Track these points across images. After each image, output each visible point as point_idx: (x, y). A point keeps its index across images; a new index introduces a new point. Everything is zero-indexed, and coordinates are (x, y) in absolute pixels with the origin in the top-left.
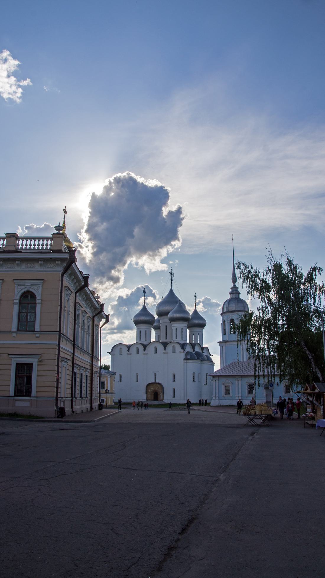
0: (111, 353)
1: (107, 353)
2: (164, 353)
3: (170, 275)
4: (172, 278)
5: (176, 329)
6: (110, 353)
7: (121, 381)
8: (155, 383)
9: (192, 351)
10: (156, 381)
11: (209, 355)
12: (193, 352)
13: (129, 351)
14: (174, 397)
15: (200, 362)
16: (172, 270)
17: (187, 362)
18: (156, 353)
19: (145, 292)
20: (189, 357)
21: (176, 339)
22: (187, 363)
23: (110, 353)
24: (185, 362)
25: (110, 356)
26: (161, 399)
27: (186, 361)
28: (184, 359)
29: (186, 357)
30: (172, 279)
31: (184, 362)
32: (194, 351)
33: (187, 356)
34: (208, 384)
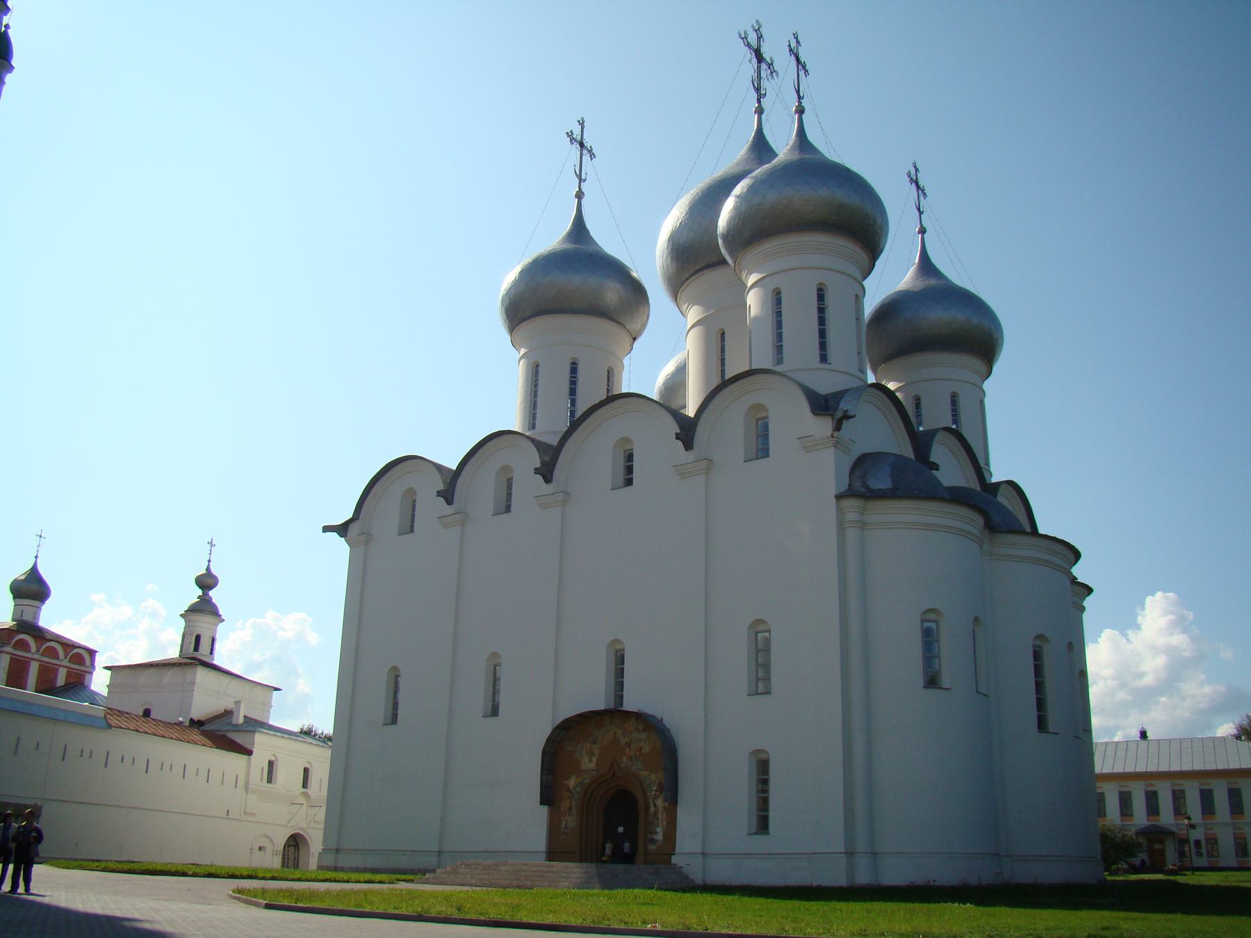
0: (353, 529)
1: (327, 529)
2: (683, 472)
3: (749, 55)
4: (759, 78)
6: (342, 530)
7: (394, 720)
8: (615, 714)
10: (619, 698)
13: (448, 495)
14: (763, 825)
15: (977, 533)
16: (760, 37)
18: (629, 482)
19: (582, 145)
21: (780, 361)
22: (863, 526)
23: (342, 530)
24: (851, 516)
25: (340, 548)
26: (652, 847)
28: (839, 497)
29: (857, 485)
30: (765, 84)
34: (1051, 728)
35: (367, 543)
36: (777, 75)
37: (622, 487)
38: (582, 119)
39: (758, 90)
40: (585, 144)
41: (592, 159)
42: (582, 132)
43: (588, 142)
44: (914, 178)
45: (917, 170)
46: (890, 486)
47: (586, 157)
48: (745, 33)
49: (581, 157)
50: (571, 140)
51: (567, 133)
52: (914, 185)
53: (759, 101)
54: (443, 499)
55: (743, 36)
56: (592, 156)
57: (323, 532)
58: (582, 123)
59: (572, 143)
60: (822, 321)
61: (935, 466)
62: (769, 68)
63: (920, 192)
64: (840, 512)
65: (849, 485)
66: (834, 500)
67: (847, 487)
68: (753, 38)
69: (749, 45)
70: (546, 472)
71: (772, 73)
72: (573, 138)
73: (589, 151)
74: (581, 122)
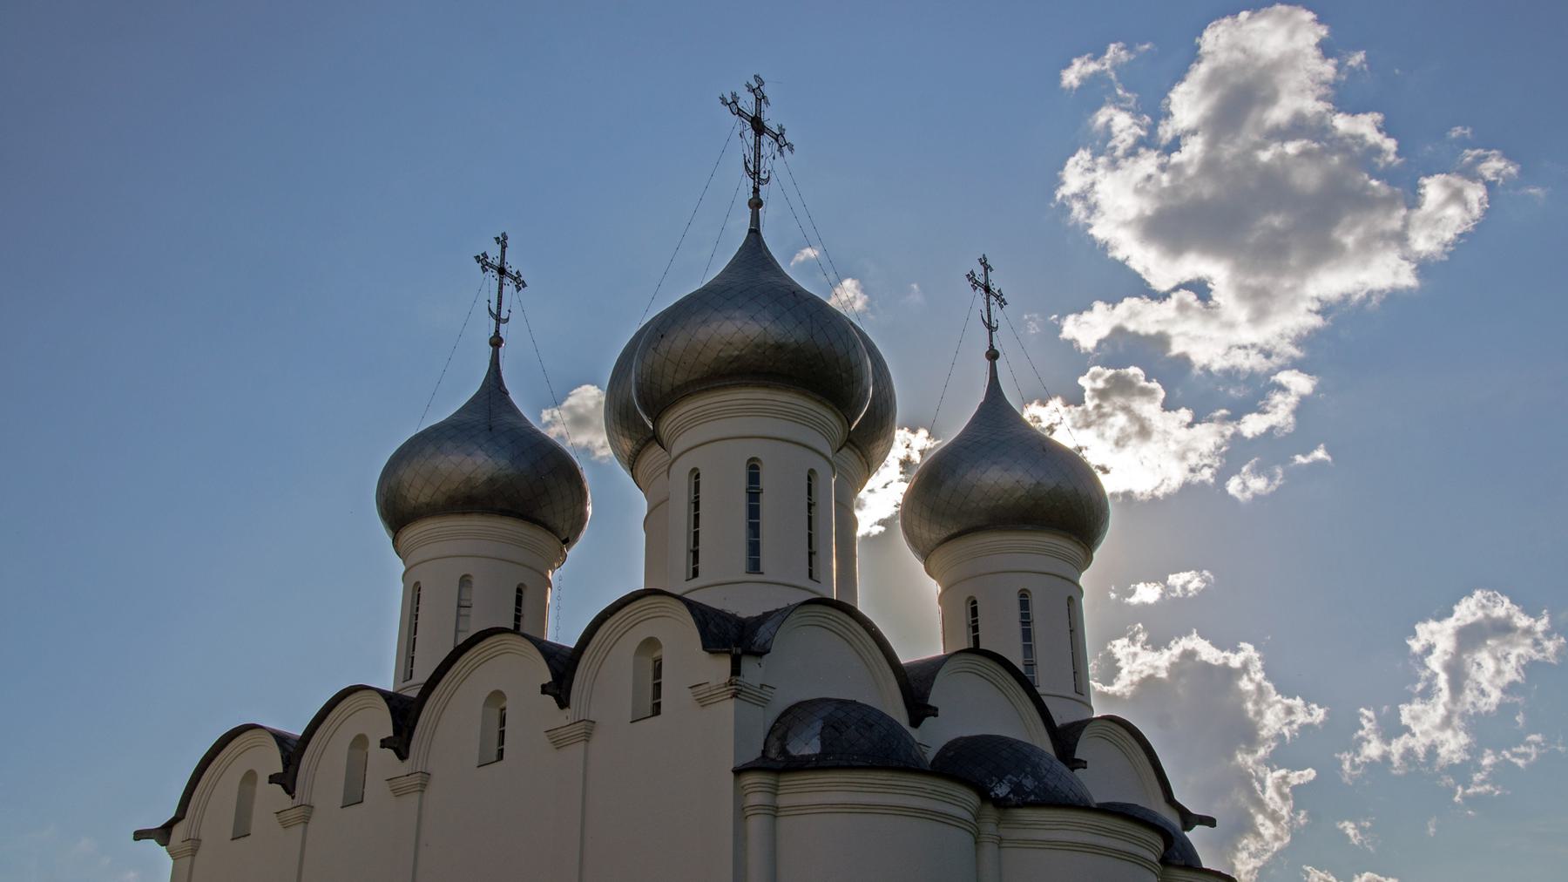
0: (178, 832)
1: (140, 835)
2: (558, 740)
4: (758, 156)
5: (696, 475)
6: (163, 834)
9: (899, 714)
11: (1174, 820)
12: (915, 722)
13: (286, 780)
16: (760, 99)
17: (783, 801)
19: (502, 271)
20: (807, 745)
22: (774, 812)
23: (163, 834)
24: (755, 799)
27: (775, 791)
29: (773, 753)
30: (766, 165)
31: (741, 813)
32: (919, 708)
33: (783, 739)
35: (194, 852)
36: (791, 149)
37: (496, 761)
38: (505, 237)
39: (755, 174)
40: (508, 270)
41: (519, 289)
42: (503, 252)
43: (512, 265)
44: (982, 280)
45: (987, 268)
46: (818, 750)
47: (509, 288)
48: (734, 95)
49: (501, 288)
50: (483, 267)
51: (477, 257)
52: (980, 292)
53: (756, 191)
54: (280, 786)
55: (730, 101)
56: (520, 284)
57: (135, 840)
58: (502, 241)
59: (485, 270)
60: (754, 512)
61: (934, 712)
62: (777, 140)
63: (993, 299)
64: (739, 794)
65: (763, 752)
66: (732, 775)
67: (759, 754)
68: (747, 103)
69: (740, 113)
70: (400, 742)
71: (781, 146)
72: (487, 264)
73: (515, 279)
74: (501, 239)
